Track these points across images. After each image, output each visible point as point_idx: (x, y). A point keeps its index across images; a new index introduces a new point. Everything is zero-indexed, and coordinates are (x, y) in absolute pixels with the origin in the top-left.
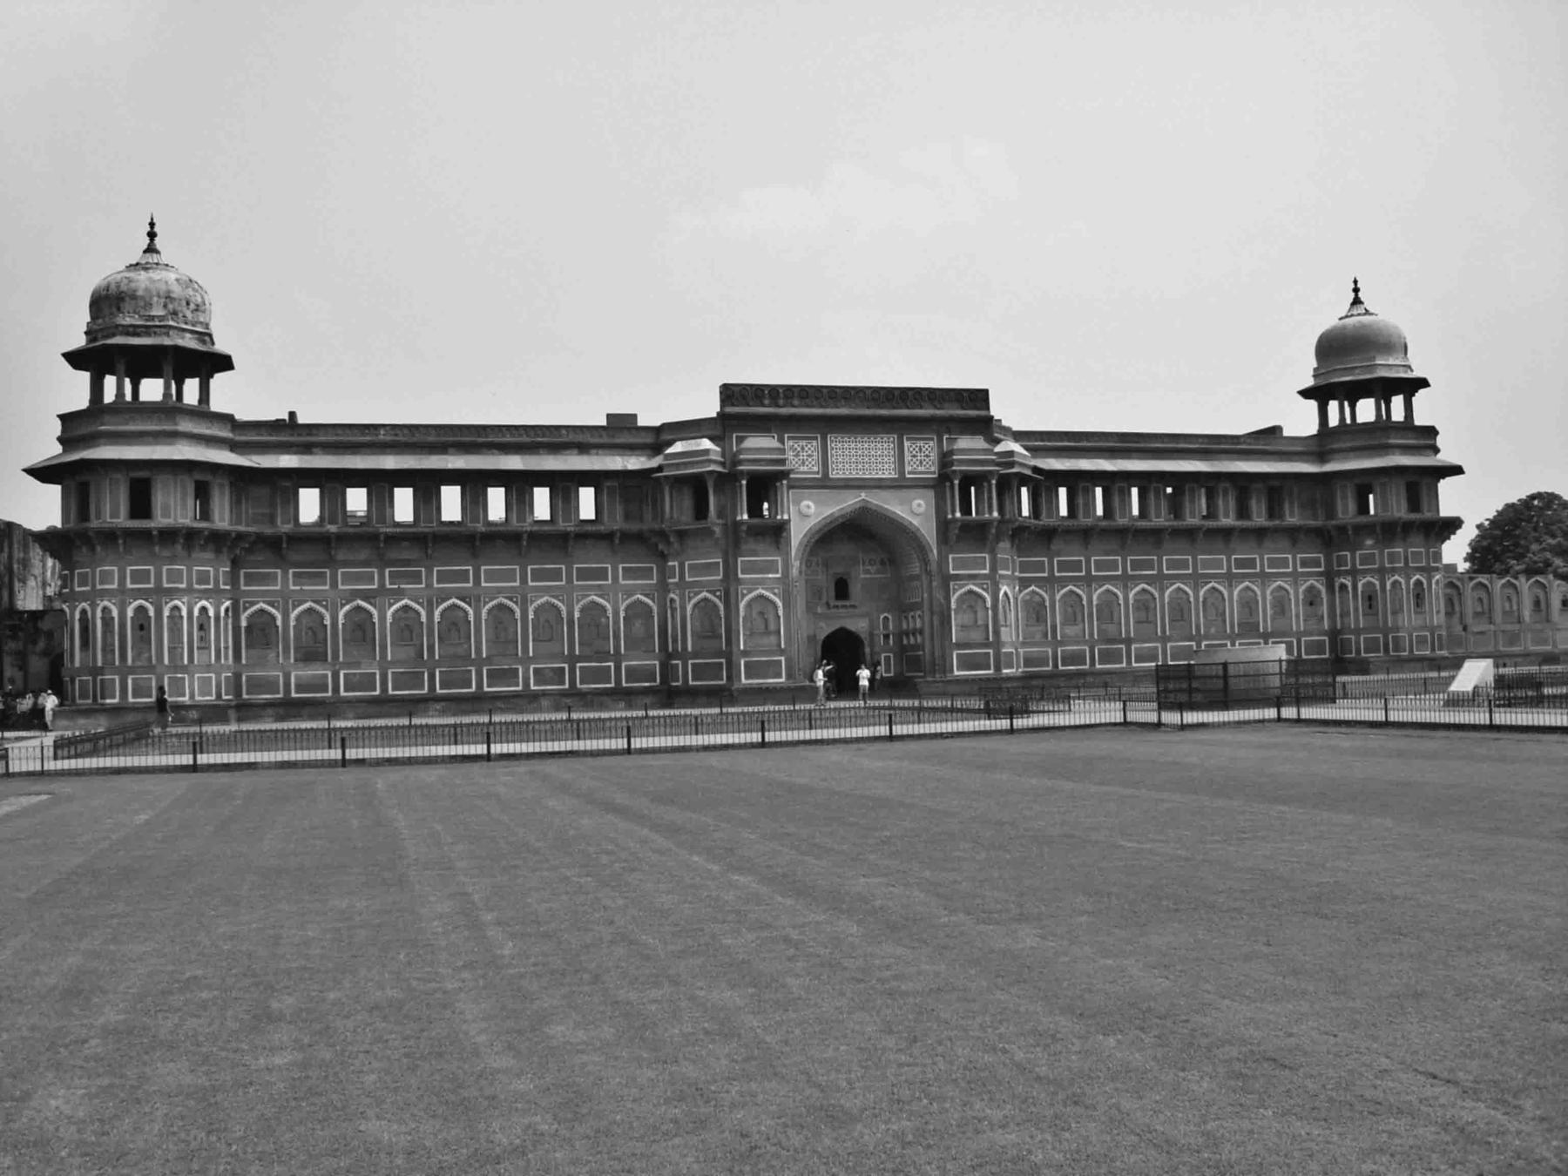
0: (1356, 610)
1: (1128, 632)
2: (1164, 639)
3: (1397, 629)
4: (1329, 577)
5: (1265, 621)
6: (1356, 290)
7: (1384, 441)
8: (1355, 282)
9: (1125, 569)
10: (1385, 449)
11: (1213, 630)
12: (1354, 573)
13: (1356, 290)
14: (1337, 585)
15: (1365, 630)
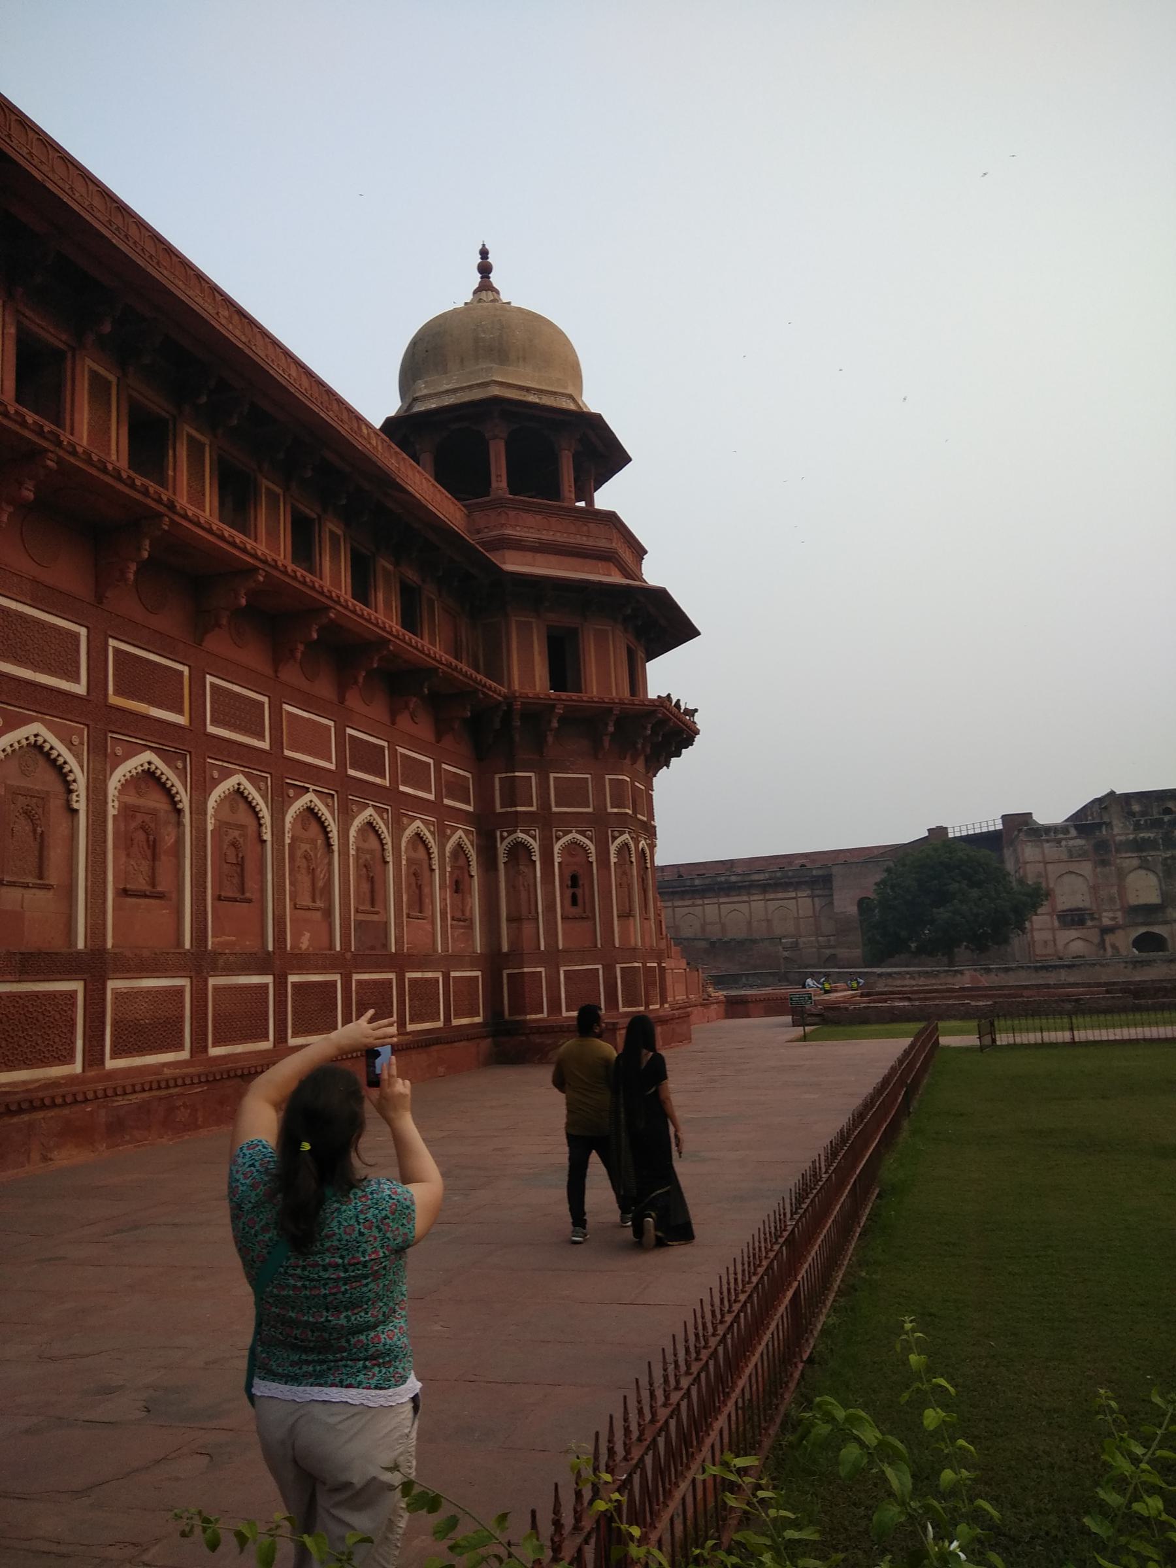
0: (550, 908)
1: (96, 930)
2: (200, 963)
3: (631, 952)
4: (486, 827)
5: (399, 925)
6: (485, 269)
7: (603, 543)
8: (484, 253)
9: (97, 682)
10: (607, 557)
11: (305, 943)
12: (545, 821)
13: (485, 269)
14: (502, 848)
15: (569, 955)
